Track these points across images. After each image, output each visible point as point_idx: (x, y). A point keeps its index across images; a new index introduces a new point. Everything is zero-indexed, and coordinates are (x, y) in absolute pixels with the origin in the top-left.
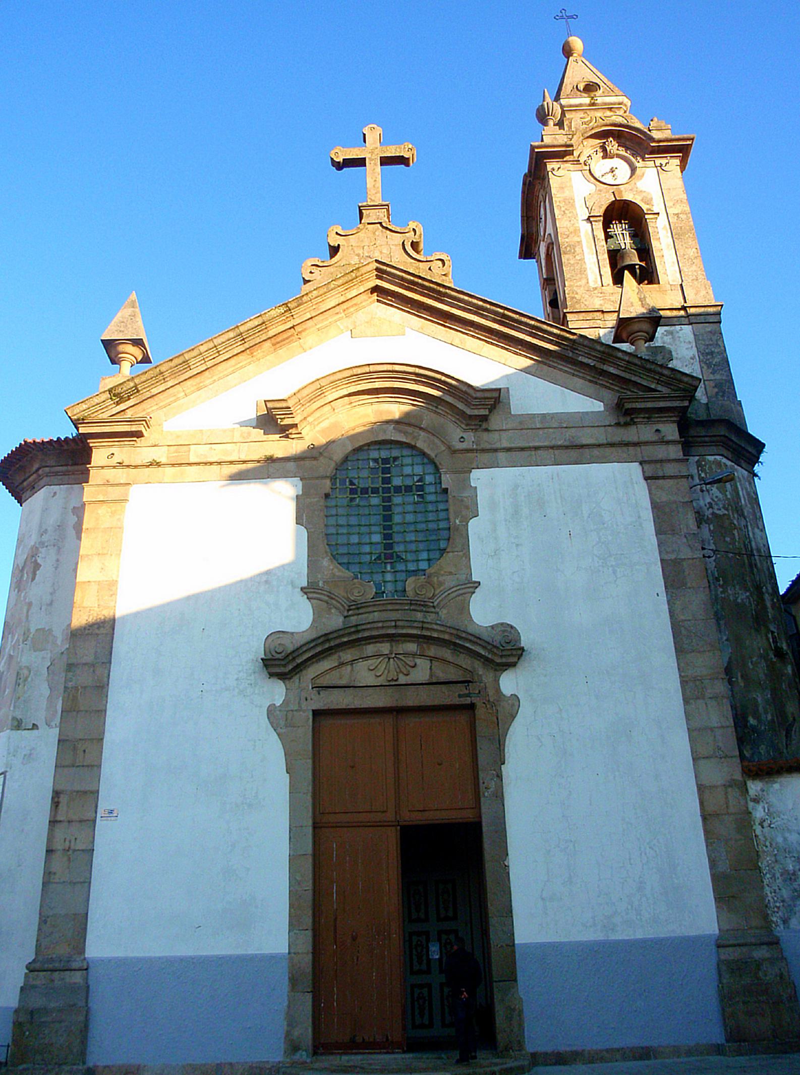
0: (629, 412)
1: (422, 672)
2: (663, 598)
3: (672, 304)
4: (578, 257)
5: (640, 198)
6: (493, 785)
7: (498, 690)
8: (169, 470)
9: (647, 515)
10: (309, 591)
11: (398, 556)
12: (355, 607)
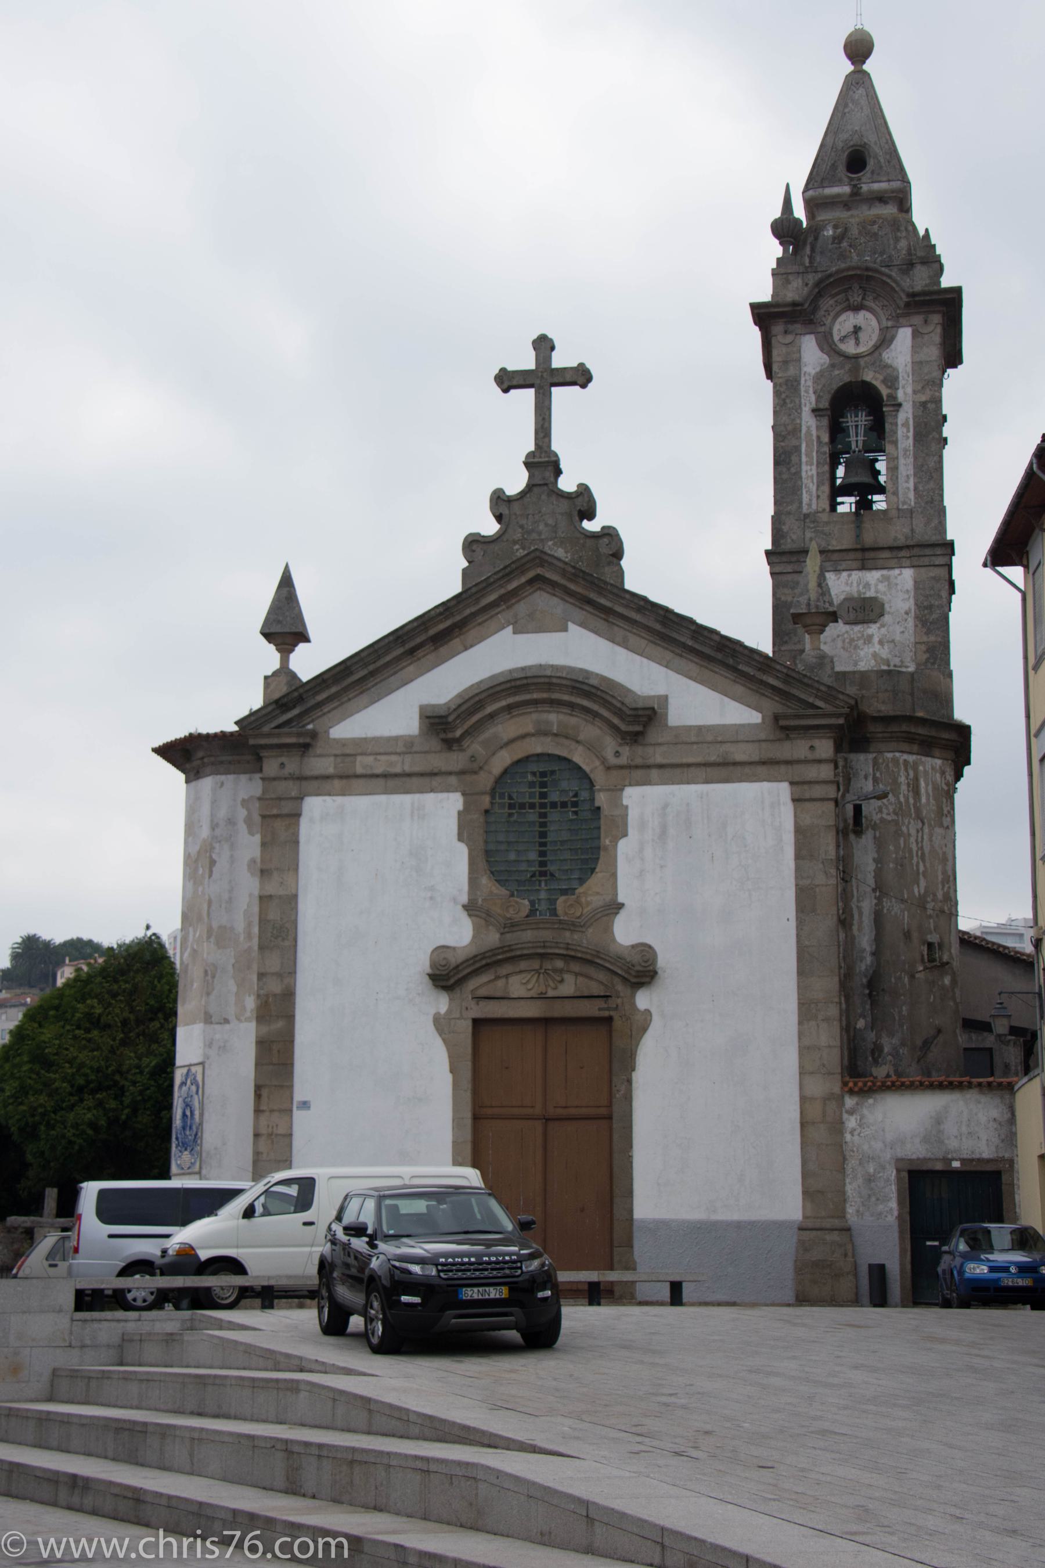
2: (793, 923)
3: (896, 539)
4: (793, 470)
5: (881, 377)
6: (623, 1088)
7: (633, 1005)
10: (470, 908)
11: (552, 875)
12: (511, 926)
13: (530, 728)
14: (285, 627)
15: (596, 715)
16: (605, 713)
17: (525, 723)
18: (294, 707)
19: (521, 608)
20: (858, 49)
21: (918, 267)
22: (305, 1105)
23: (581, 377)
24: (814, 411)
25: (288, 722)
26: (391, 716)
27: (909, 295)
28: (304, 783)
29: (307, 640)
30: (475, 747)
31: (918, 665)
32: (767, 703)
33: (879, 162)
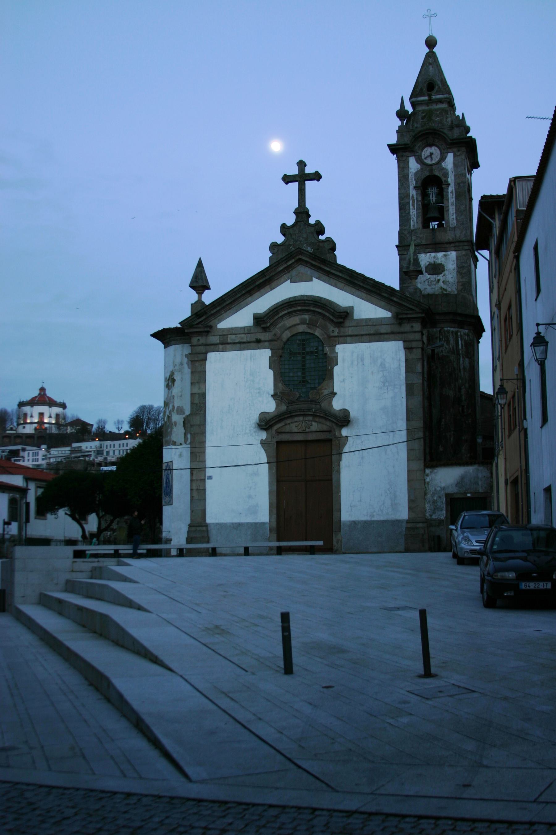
0: (401, 319)
1: (315, 426)
3: (449, 239)
4: (407, 212)
8: (221, 347)
9: (403, 364)
10: (274, 396)
11: (307, 382)
13: (298, 322)
14: (199, 283)
15: (324, 316)
16: (327, 314)
17: (295, 320)
18: (202, 316)
19: (294, 273)
20: (431, 43)
21: (455, 128)
22: (210, 477)
23: (317, 176)
24: (415, 187)
25: (201, 322)
26: (241, 318)
27: (451, 140)
28: (208, 347)
29: (209, 289)
30: (277, 330)
31: (458, 291)
32: (394, 309)
33: (439, 87)
